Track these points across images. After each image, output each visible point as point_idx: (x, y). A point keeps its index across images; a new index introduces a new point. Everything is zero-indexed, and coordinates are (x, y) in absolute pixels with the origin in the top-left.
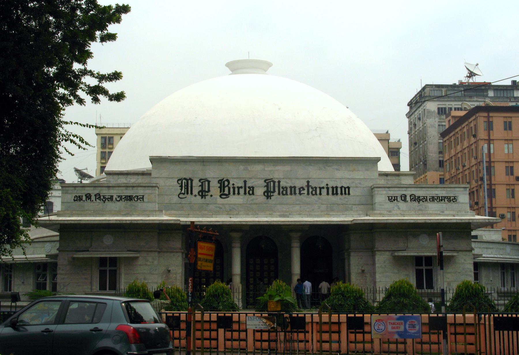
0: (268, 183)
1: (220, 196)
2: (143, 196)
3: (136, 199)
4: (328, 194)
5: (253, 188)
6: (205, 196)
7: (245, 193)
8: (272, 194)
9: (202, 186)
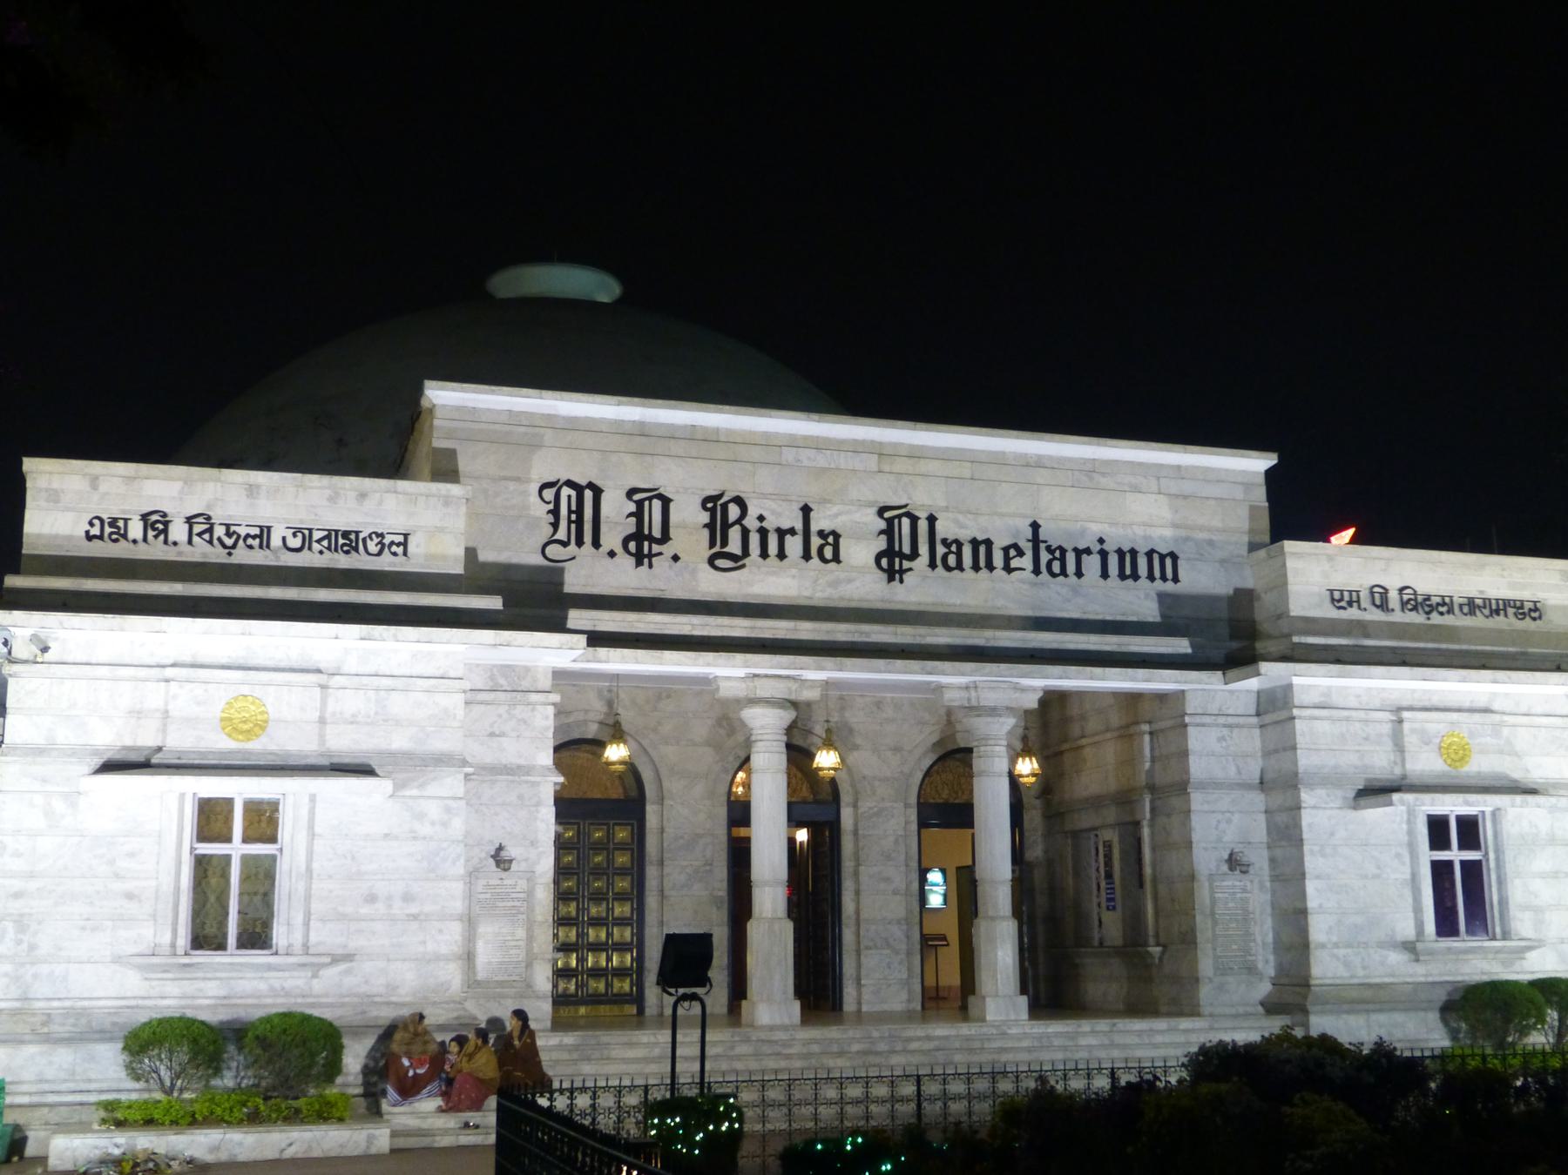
0: (890, 521)
1: (711, 561)
2: (406, 536)
3: (373, 547)
4: (1105, 574)
5: (836, 536)
6: (650, 556)
7: (807, 556)
8: (906, 564)
9: (638, 515)
